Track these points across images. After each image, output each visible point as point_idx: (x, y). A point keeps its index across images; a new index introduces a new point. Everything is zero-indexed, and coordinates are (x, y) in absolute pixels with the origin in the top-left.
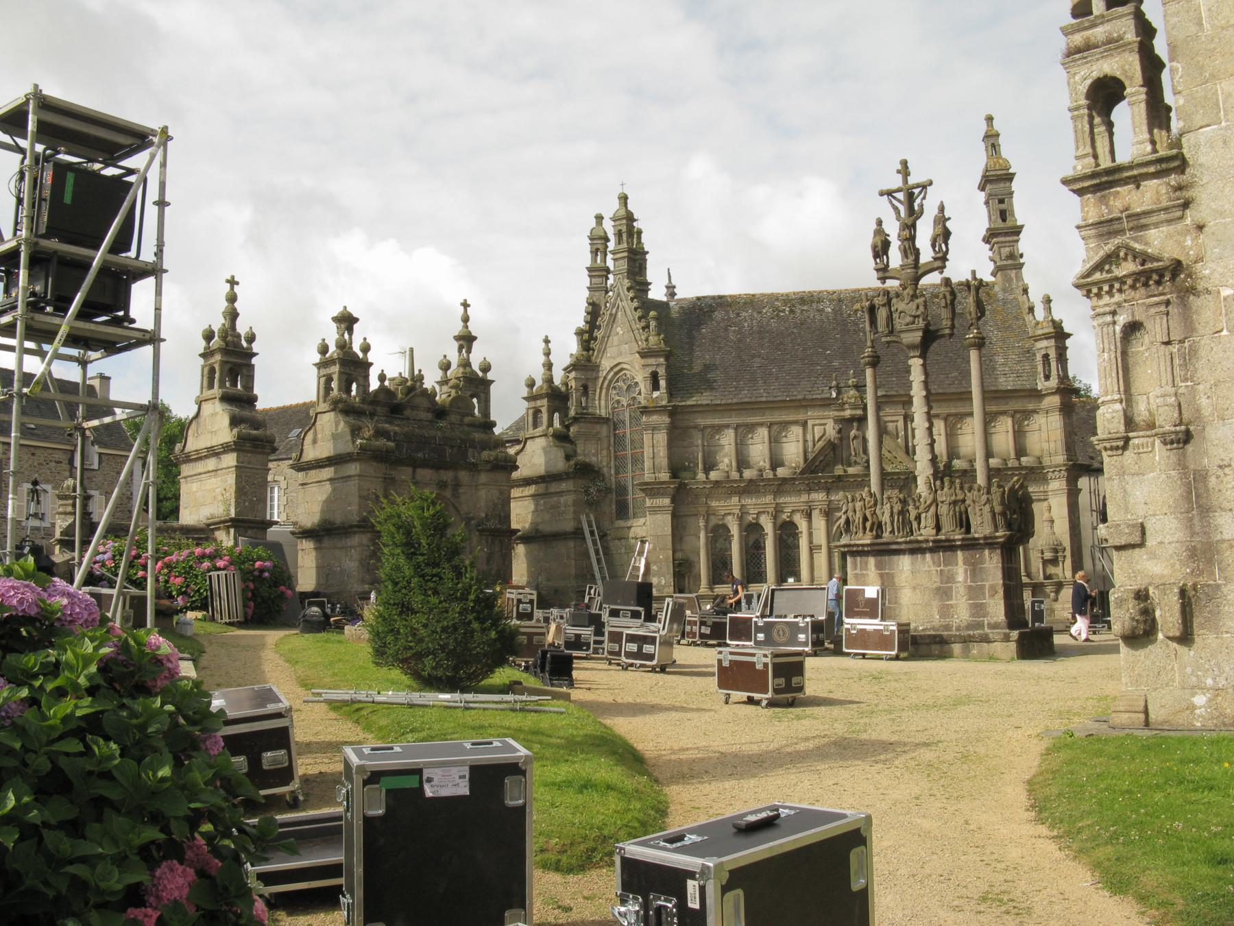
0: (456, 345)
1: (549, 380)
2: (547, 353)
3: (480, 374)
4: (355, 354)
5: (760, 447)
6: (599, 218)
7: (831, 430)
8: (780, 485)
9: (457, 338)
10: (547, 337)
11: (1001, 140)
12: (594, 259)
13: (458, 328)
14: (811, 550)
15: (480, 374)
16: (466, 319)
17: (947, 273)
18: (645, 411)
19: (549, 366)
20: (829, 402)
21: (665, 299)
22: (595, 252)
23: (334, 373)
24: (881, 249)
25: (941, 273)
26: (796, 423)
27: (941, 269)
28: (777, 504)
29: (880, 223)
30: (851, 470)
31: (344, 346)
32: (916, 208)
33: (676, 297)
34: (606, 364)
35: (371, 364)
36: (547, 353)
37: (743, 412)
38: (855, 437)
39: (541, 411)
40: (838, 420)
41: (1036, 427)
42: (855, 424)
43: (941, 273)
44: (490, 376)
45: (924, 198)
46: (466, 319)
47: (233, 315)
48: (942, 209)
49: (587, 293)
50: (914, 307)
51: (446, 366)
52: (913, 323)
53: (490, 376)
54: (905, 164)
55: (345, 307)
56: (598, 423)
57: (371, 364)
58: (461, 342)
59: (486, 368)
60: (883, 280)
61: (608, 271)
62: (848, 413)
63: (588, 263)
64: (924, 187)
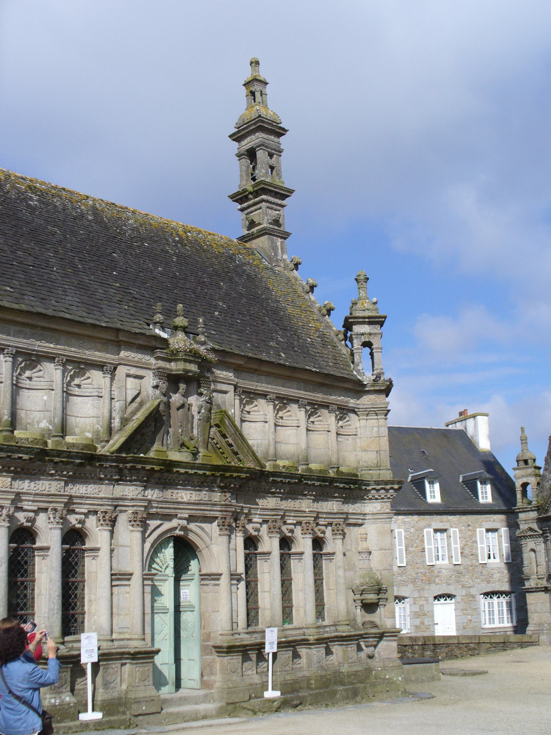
5: (43, 396)
8: (81, 464)
11: (268, 89)
20: (153, 343)
26: (100, 366)
28: (71, 497)
30: (175, 456)
37: (28, 330)
38: (182, 406)
40: (160, 373)
62: (176, 367)
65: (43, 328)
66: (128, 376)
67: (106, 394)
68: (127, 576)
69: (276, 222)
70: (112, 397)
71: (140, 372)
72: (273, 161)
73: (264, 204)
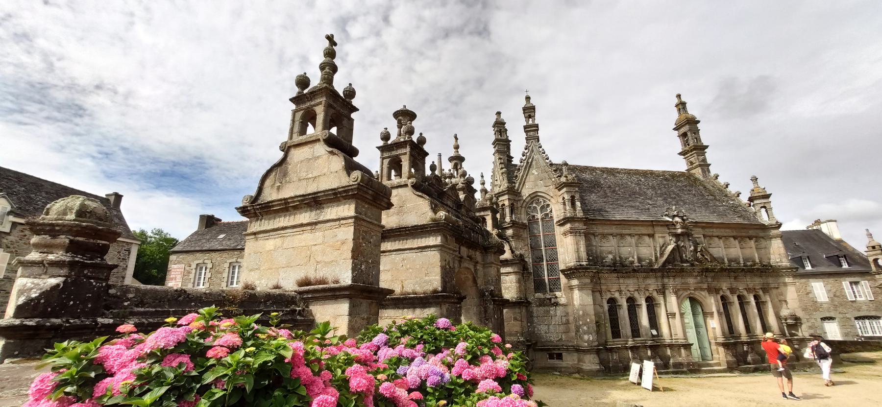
14: (668, 316)
16: (457, 147)
34: (526, 192)
41: (763, 246)
46: (457, 147)
47: (329, 68)
56: (521, 228)
58: (455, 161)
65: (624, 225)
66: (659, 237)
67: (652, 245)
68: (674, 315)
69: (704, 160)
71: (663, 235)
72: (696, 136)
73: (695, 155)
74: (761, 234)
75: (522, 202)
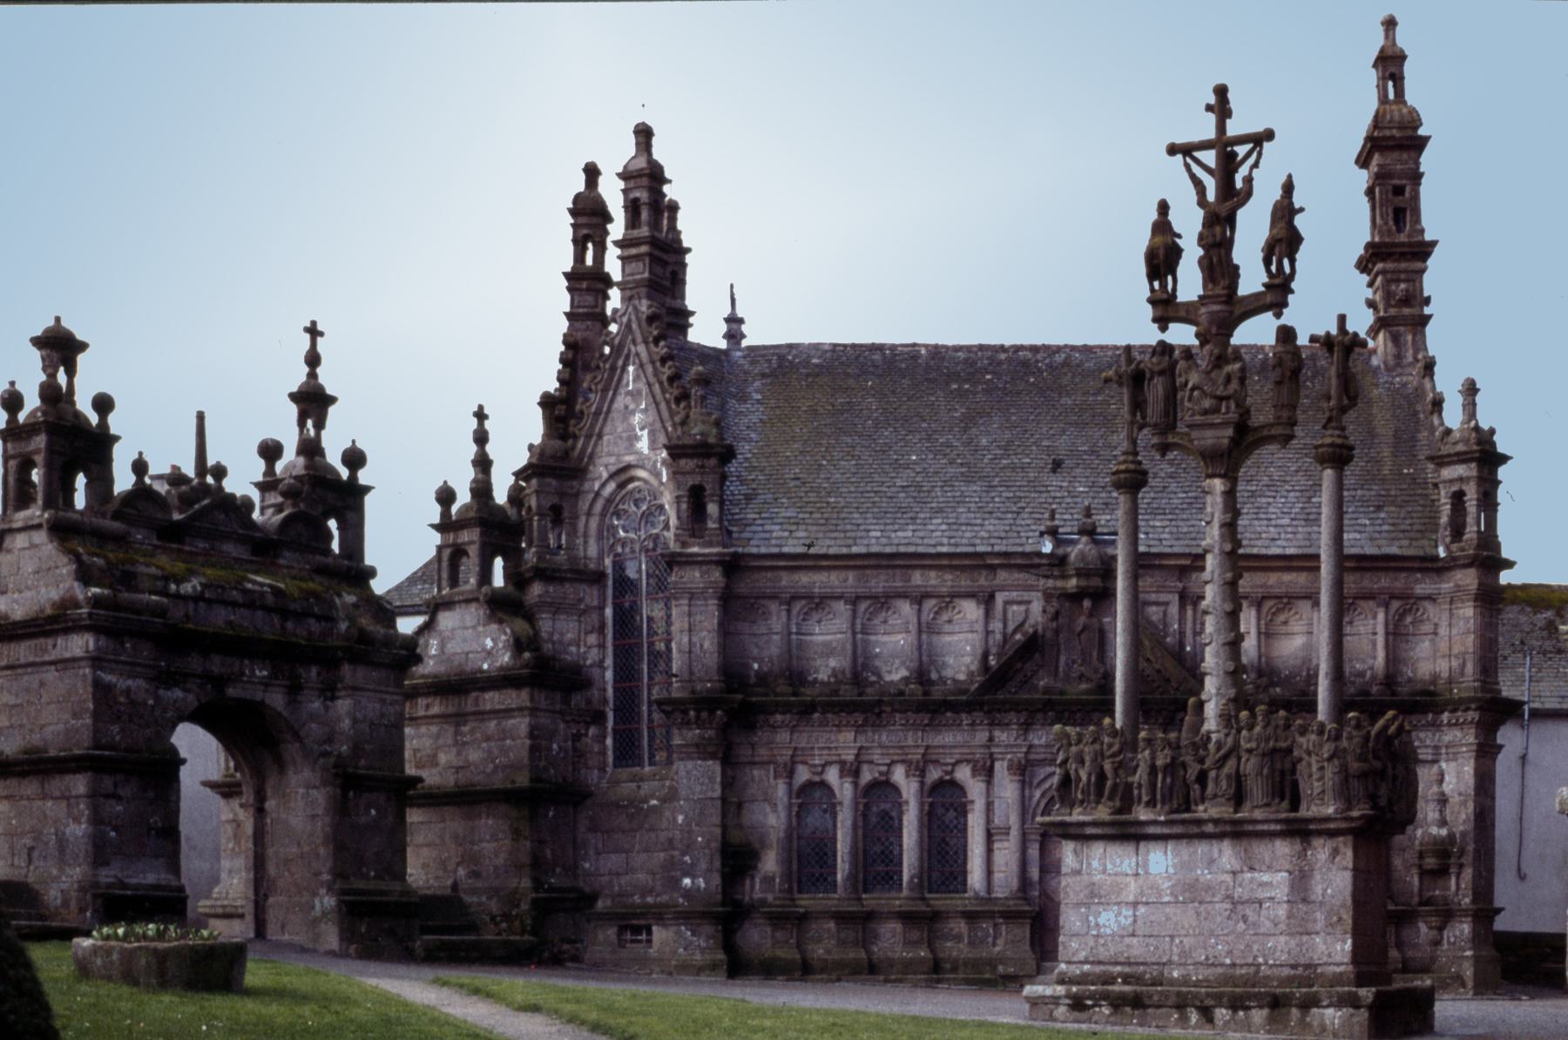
0: (293, 410)
1: (482, 490)
2: (481, 438)
3: (344, 473)
4: (78, 415)
6: (592, 172)
7: (1035, 611)
9: (294, 397)
10: (481, 407)
12: (579, 257)
13: (297, 376)
15: (344, 473)
16: (313, 360)
17: (1289, 317)
18: (673, 561)
19: (483, 463)
21: (722, 344)
22: (579, 244)
23: (37, 451)
24: (1162, 260)
25: (1278, 315)
27: (1279, 307)
29: (1163, 207)
31: (54, 397)
32: (1239, 184)
33: (745, 343)
35: (116, 438)
36: (481, 438)
39: (465, 553)
42: (1087, 603)
43: (1278, 315)
44: (363, 477)
45: (1256, 165)
46: (313, 360)
48: (1288, 188)
49: (564, 325)
50: (1221, 380)
51: (271, 451)
52: (1216, 410)
53: (363, 477)
54: (1221, 92)
55: (58, 319)
57: (116, 438)
59: (355, 459)
60: (1162, 322)
61: (607, 281)
63: (568, 265)
64: (1259, 140)
70: (990, 629)
74: (1419, 589)
75: (591, 496)
